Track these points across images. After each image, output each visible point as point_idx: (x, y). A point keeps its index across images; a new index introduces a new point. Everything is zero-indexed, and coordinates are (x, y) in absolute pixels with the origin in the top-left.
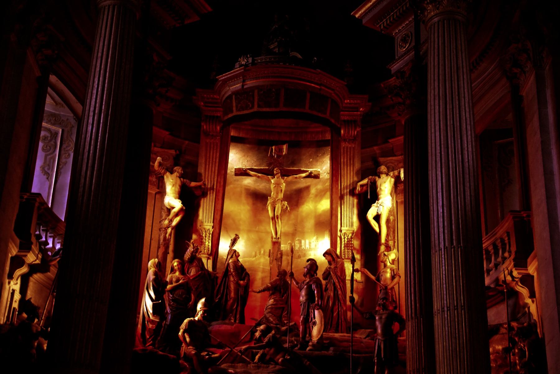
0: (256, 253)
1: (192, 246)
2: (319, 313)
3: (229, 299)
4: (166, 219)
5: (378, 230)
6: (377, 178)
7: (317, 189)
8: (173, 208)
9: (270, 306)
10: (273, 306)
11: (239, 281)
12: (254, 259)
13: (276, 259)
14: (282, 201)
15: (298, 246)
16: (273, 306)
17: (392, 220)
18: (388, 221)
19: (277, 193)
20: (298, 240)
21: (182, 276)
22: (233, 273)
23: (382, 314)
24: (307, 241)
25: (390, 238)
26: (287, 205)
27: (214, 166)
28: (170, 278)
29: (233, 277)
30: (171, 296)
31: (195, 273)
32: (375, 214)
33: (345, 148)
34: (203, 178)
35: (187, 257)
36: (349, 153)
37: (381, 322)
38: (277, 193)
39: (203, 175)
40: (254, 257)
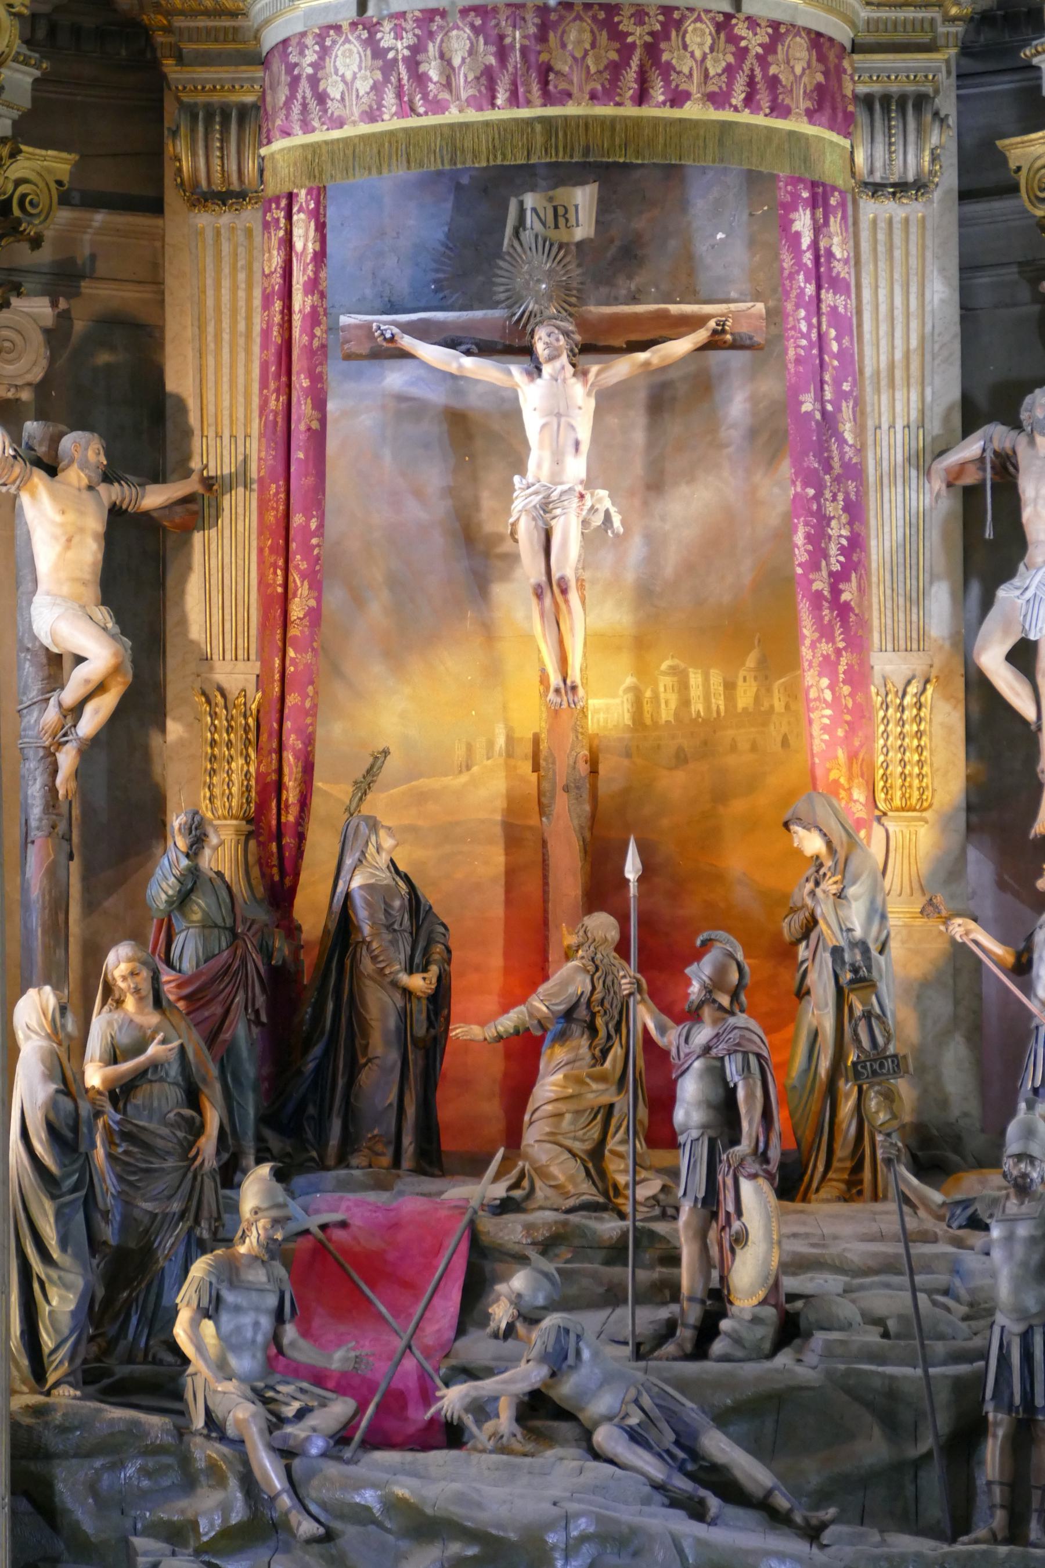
0: (470, 748)
2: (758, 1191)
3: (363, 1061)
6: (1022, 441)
7: (753, 399)
8: (80, 660)
9: (549, 1108)
10: (561, 1107)
12: (464, 778)
13: (566, 789)
15: (673, 699)
16: (561, 1107)
19: (558, 460)
20: (674, 670)
21: (153, 1019)
23: (1014, 1220)
26: (607, 503)
27: (242, 356)
28: (104, 1036)
30: (118, 1117)
33: (882, 225)
34: (193, 419)
35: (164, 897)
36: (897, 254)
37: (1010, 1256)
38: (558, 460)
39: (192, 404)
40: (461, 772)
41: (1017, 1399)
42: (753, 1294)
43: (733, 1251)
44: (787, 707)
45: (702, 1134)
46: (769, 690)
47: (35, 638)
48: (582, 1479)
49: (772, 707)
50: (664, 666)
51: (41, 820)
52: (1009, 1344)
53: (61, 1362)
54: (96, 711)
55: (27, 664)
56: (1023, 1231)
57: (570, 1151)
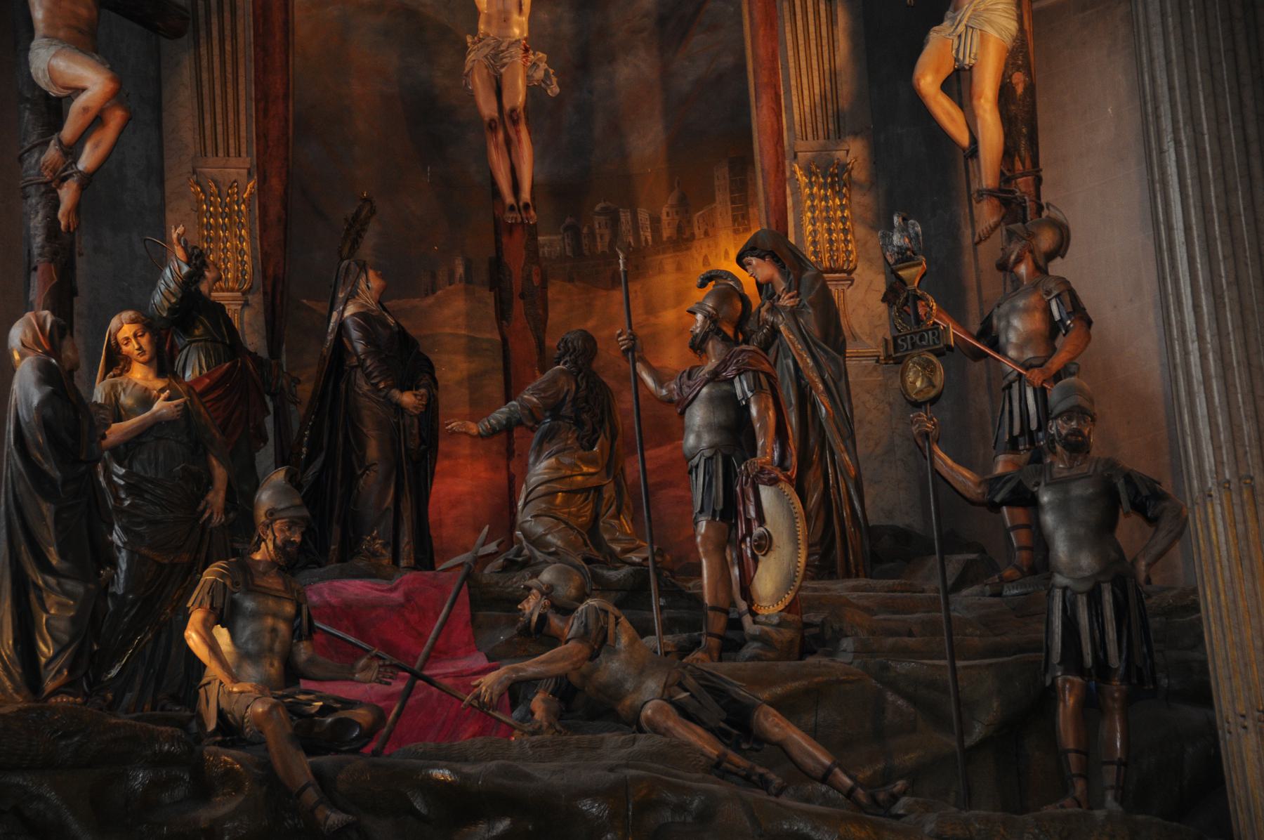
1: (180, 253)
2: (780, 495)
4: (47, 144)
5: (963, 138)
11: (396, 393)
12: (430, 300)
13: (522, 296)
14: (526, 50)
16: (556, 486)
17: (1020, 89)
18: (1005, 93)
19: (506, 20)
21: (159, 384)
22: (368, 362)
24: (643, 215)
25: (1019, 166)
26: (543, 66)
29: (368, 376)
30: (122, 471)
31: (205, 371)
32: (947, 69)
40: (427, 295)
41: (1088, 660)
42: (778, 600)
43: (755, 559)
44: (706, 234)
45: (715, 453)
46: (689, 222)
47: (34, 85)
48: (636, 747)
49: (693, 235)
50: (597, 208)
51: (43, 247)
52: (1074, 605)
53: (59, 671)
54: (96, 146)
55: (27, 114)
56: (1078, 490)
57: (567, 524)
